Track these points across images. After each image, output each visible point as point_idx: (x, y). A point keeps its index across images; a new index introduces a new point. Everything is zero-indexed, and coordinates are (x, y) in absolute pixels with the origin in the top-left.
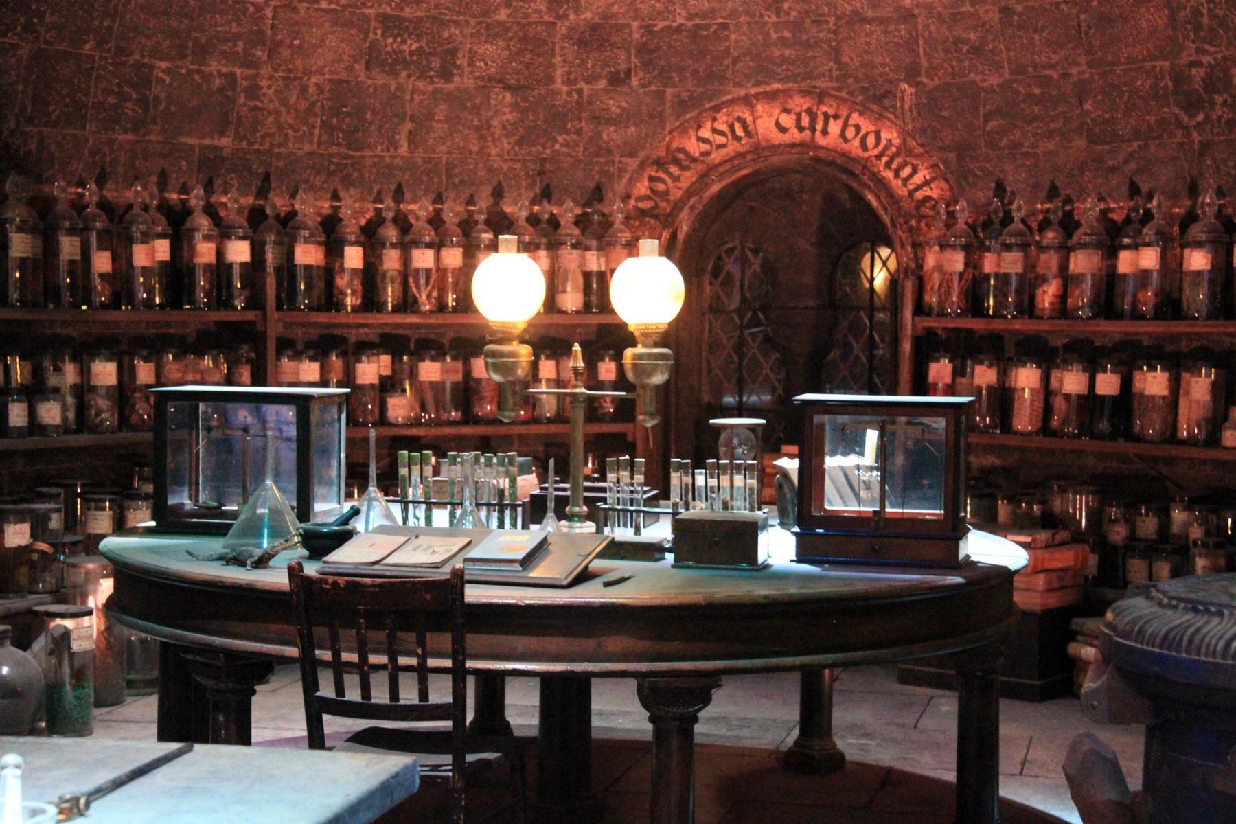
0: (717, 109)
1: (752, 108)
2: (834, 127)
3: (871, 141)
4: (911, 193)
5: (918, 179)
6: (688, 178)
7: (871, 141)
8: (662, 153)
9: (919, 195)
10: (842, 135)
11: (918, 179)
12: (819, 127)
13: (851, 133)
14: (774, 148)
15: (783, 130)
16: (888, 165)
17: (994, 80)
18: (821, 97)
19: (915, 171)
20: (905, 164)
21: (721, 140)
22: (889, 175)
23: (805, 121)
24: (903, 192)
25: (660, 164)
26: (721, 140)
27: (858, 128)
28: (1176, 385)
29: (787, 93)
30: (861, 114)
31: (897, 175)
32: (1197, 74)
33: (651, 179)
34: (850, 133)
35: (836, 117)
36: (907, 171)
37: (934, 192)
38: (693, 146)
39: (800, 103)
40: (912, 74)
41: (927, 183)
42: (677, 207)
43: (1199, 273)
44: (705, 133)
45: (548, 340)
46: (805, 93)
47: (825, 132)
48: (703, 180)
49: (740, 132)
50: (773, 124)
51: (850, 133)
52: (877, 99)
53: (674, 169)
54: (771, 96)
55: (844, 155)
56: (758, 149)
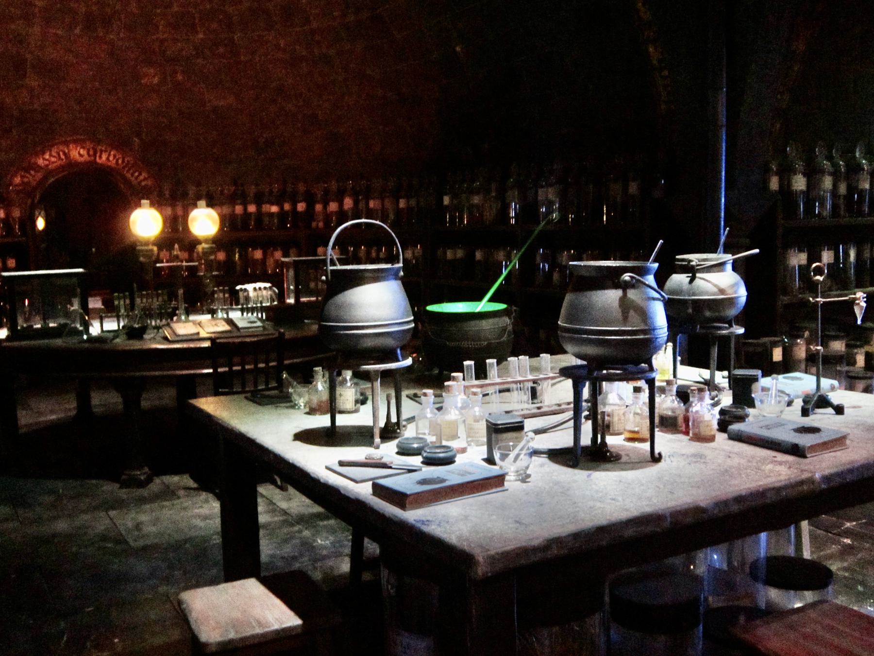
0: (52, 146)
1: (68, 146)
2: (104, 157)
3: (120, 161)
4: (140, 183)
5: (141, 177)
6: (39, 176)
7: (120, 161)
8: (25, 165)
9: (143, 184)
10: (108, 159)
11: (141, 177)
12: (98, 155)
13: (107, 158)
14: (77, 164)
15: (81, 156)
16: (128, 171)
17: (174, 139)
18: (99, 142)
19: (140, 174)
20: (135, 172)
21: (53, 159)
22: (129, 175)
23: (91, 153)
24: (135, 182)
25: (27, 170)
26: (53, 159)
27: (115, 156)
28: (265, 254)
29: (83, 141)
30: (117, 150)
31: (132, 175)
32: (262, 141)
33: (22, 177)
34: (111, 158)
35: (106, 151)
36: (136, 174)
37: (149, 182)
38: (40, 162)
39: (88, 144)
40: (138, 135)
41: (145, 179)
42: (35, 189)
43: (273, 213)
44: (47, 156)
45: (165, 242)
46: (92, 141)
47: (100, 157)
48: (45, 178)
49: (63, 157)
50: (78, 153)
51: (111, 158)
52: (120, 144)
53: (32, 172)
54: (75, 142)
55: (108, 167)
56: (71, 164)
